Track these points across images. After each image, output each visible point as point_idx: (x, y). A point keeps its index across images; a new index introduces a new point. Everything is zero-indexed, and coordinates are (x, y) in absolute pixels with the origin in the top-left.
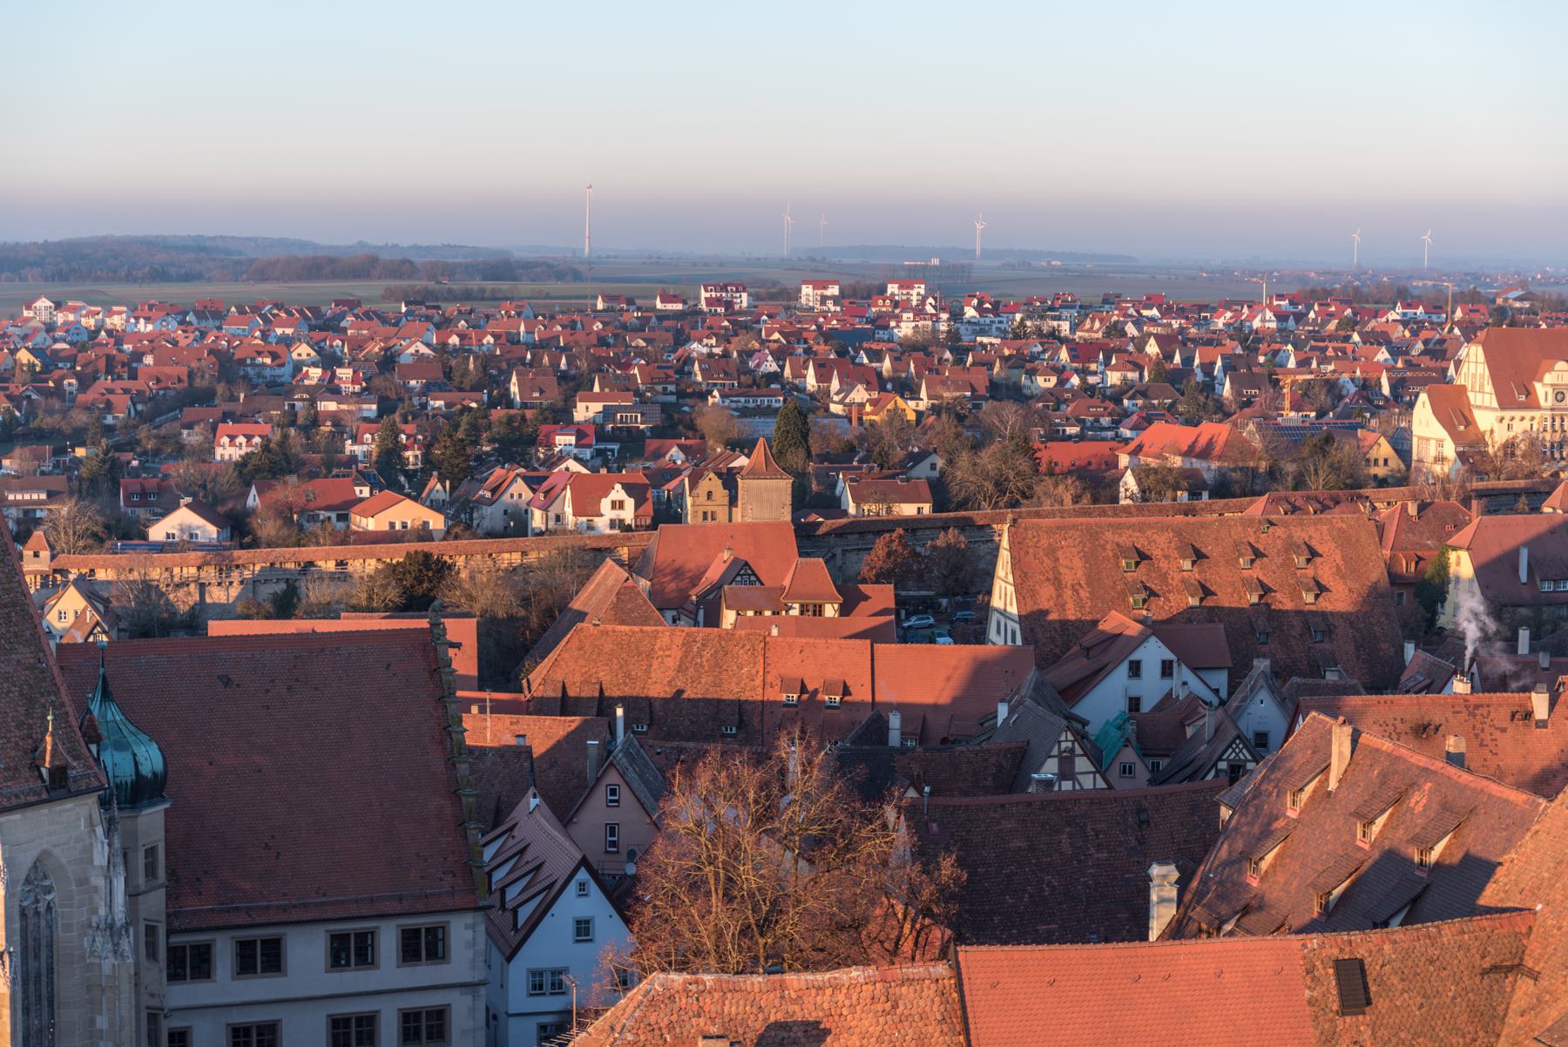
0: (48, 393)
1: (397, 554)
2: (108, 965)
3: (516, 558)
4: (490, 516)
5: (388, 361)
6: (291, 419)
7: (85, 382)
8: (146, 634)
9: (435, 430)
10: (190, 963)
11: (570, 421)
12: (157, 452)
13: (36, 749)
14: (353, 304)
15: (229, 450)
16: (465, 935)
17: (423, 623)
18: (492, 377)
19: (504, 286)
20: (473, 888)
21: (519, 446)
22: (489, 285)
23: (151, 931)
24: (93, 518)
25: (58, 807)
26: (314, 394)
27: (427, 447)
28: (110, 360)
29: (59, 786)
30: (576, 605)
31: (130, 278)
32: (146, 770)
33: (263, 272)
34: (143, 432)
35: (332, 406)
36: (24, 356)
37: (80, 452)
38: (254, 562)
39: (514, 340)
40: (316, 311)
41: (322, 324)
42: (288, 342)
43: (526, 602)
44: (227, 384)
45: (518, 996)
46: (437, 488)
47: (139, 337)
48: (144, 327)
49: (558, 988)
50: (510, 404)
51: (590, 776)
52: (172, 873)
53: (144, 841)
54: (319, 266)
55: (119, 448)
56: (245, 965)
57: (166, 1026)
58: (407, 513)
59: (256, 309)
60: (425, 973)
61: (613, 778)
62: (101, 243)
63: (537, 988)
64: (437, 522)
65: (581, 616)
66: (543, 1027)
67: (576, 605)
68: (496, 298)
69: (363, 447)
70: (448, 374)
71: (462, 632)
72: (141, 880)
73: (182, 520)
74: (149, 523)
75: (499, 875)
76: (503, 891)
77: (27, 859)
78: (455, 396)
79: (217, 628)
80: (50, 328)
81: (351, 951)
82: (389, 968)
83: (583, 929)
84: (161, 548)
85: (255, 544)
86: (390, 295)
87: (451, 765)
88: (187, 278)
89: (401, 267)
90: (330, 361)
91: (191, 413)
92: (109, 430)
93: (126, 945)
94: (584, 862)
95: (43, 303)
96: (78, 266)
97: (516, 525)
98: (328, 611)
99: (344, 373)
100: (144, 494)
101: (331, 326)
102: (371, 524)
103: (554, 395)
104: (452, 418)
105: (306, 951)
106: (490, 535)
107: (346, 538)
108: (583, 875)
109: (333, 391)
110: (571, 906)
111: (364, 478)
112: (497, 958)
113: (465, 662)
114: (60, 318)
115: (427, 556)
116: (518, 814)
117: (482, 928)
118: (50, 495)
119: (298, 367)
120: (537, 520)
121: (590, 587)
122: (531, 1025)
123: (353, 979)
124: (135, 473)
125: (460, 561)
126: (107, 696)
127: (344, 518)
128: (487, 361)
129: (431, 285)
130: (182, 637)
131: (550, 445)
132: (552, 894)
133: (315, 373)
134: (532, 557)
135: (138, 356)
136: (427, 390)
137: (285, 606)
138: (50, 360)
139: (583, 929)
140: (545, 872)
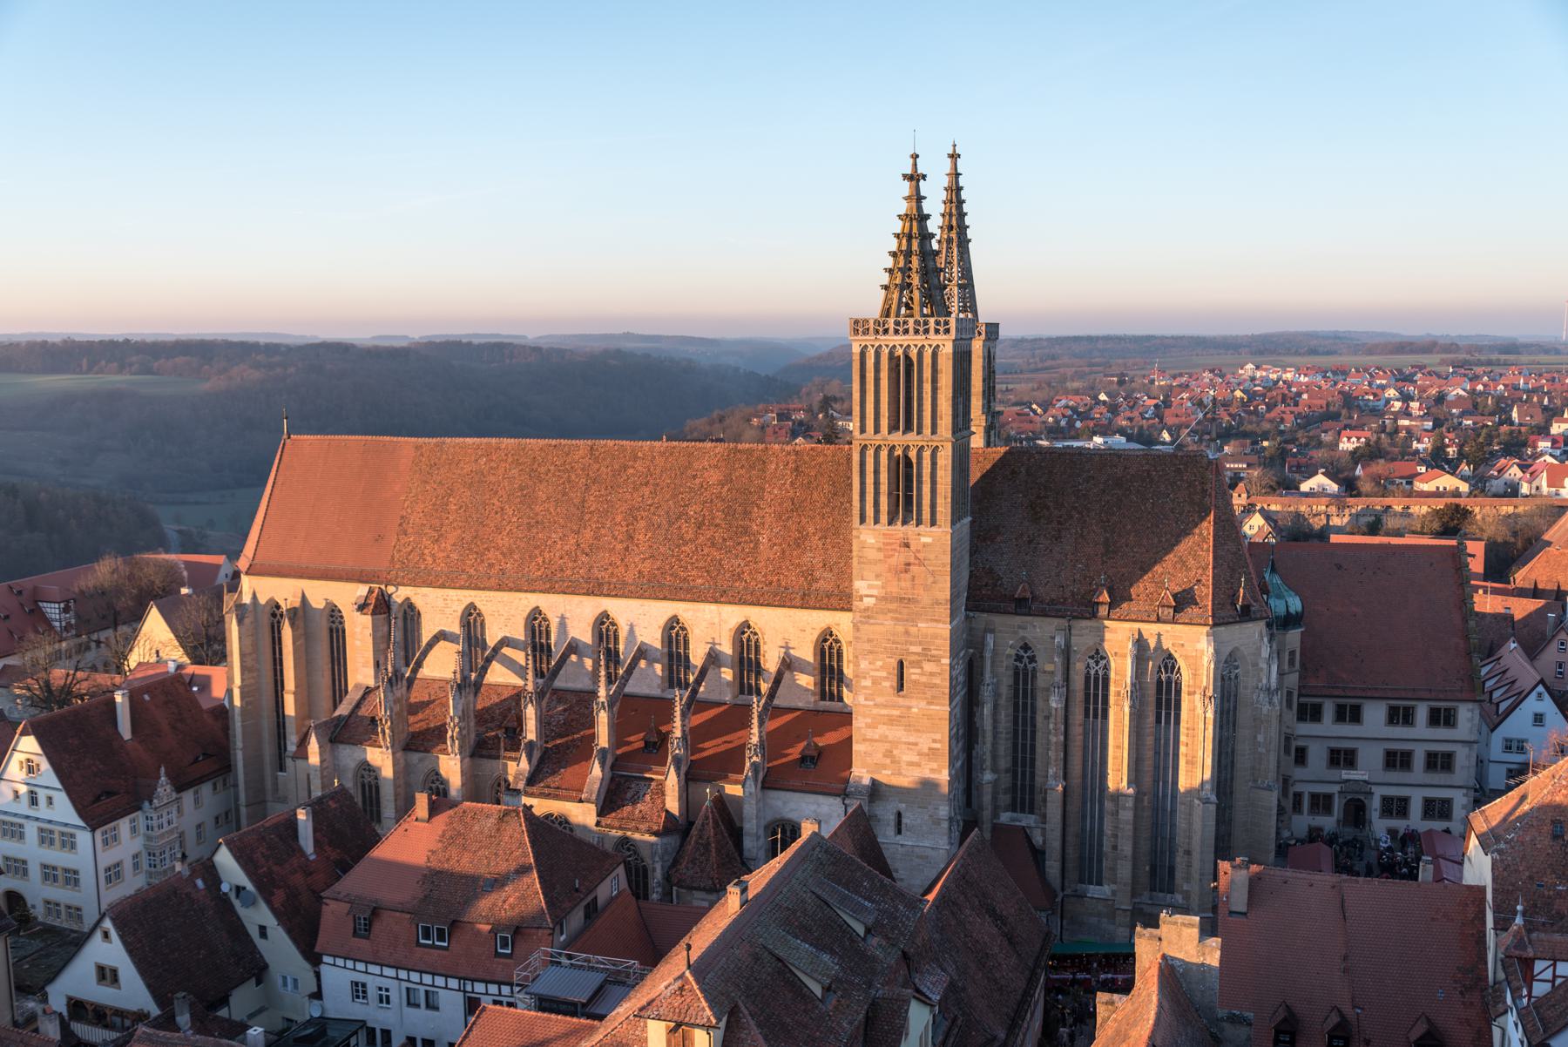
0: (1250, 413)
1: (1440, 504)
2: (1265, 709)
3: (1511, 509)
4: (1496, 485)
5: (1441, 399)
6: (1383, 429)
7: (1270, 407)
8: (1296, 540)
9: (1465, 437)
10: (1310, 713)
11: (1548, 434)
12: (1307, 445)
13: (1235, 595)
14: (1421, 368)
15: (1347, 445)
16: (1467, 715)
17: (1454, 543)
18: (1502, 408)
19: (1512, 357)
20: (1474, 690)
21: (1516, 447)
22: (1503, 357)
23: (1290, 694)
24: (1271, 478)
25: (1244, 625)
26: (1397, 416)
27: (1461, 447)
28: (1284, 396)
29: (1246, 615)
30: (1546, 537)
31: (1297, 353)
32: (1292, 610)
33: (1371, 350)
34: (1300, 434)
35: (1406, 422)
36: (1238, 394)
37: (1266, 444)
38: (1358, 504)
39: (1516, 388)
40: (1400, 371)
41: (1403, 378)
42: (1383, 388)
43: (1515, 534)
44: (1347, 411)
45: (1496, 750)
46: (1465, 468)
47: (1301, 384)
48: (1303, 379)
49: (1521, 749)
50: (1512, 423)
51: (1549, 634)
52: (1303, 665)
53: (1289, 648)
54: (1404, 347)
55: (1286, 442)
56: (1340, 716)
57: (1294, 744)
58: (1447, 482)
59: (1366, 370)
60: (1442, 733)
61: (1563, 636)
62: (1282, 335)
63: (1508, 748)
64: (1464, 487)
65: (1549, 544)
66: (1510, 771)
67: (1546, 537)
68: (1506, 364)
69: (1424, 445)
70: (1475, 406)
71: (1476, 548)
72: (1286, 667)
73: (1319, 481)
74: (1301, 482)
75: (1489, 684)
76: (1491, 693)
77: (1227, 650)
78: (1479, 418)
79: (1334, 539)
80: (1253, 379)
81: (1400, 716)
82: (1420, 726)
83: (1539, 719)
84: (1306, 495)
85: (1359, 495)
86: (1443, 362)
87: (1465, 620)
88: (1329, 353)
89: (1451, 347)
90: (1406, 398)
91: (1326, 425)
92: (1282, 432)
93: (1276, 700)
94: (1542, 682)
95: (1250, 366)
96: (1268, 347)
97: (1512, 491)
98: (1398, 533)
99: (1414, 405)
100: (1299, 466)
101: (1409, 379)
102: (1425, 487)
103: (1539, 419)
104: (1476, 430)
105: (1375, 715)
106: (1495, 496)
107: (1411, 494)
108: (1540, 688)
109: (1406, 413)
110: (1531, 705)
111: (1423, 462)
112: (1485, 729)
113: (1477, 565)
114: (1258, 374)
115: (1457, 506)
116: (1502, 651)
117: (1477, 712)
118: (1249, 465)
119: (1388, 401)
120: (1525, 489)
121: (1556, 527)
122: (1504, 768)
123: (1399, 731)
124: (1295, 455)
125: (1477, 510)
126: (1273, 570)
127: (1410, 483)
128: (1499, 399)
129: (1468, 357)
130: (1316, 542)
131: (1535, 447)
132: (1521, 698)
133: (1397, 405)
134: (1521, 509)
135: (1299, 394)
136: (1463, 415)
137: (1374, 529)
138: (1252, 395)
139: (1539, 719)
140: (1517, 684)
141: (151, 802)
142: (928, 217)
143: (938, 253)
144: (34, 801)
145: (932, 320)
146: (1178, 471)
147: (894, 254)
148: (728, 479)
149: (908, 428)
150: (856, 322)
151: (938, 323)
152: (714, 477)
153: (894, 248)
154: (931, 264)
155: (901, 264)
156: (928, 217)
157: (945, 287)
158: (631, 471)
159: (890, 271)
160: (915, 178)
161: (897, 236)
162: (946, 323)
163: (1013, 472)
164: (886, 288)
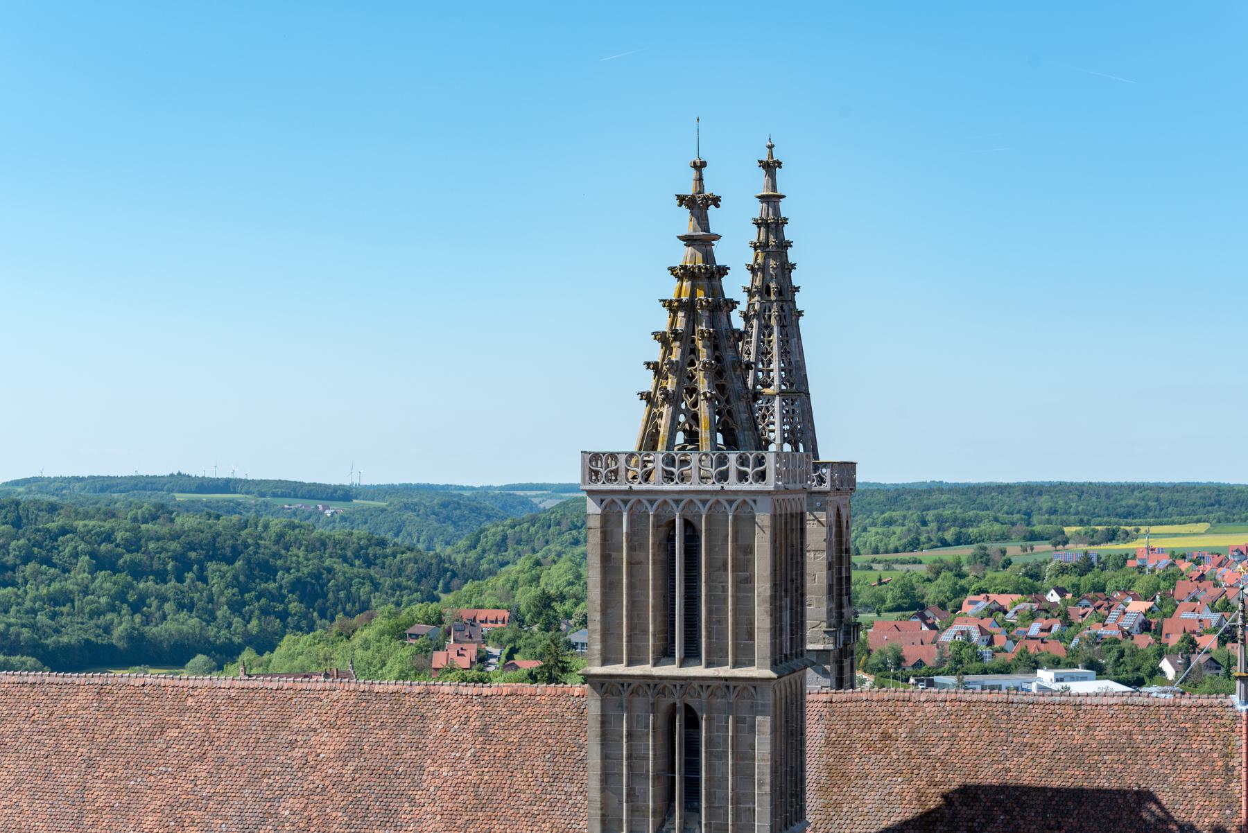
142: (723, 271)
143: (742, 335)
145: (733, 457)
146: (1183, 734)
147: (662, 338)
148: (354, 750)
149: (691, 654)
150: (595, 457)
151: (743, 461)
152: (329, 744)
153: (664, 327)
154: (729, 355)
155: (676, 356)
156: (723, 271)
157: (756, 396)
158: (173, 733)
159: (655, 367)
160: (699, 204)
161: (668, 304)
162: (760, 461)
163: (886, 736)
164: (648, 397)
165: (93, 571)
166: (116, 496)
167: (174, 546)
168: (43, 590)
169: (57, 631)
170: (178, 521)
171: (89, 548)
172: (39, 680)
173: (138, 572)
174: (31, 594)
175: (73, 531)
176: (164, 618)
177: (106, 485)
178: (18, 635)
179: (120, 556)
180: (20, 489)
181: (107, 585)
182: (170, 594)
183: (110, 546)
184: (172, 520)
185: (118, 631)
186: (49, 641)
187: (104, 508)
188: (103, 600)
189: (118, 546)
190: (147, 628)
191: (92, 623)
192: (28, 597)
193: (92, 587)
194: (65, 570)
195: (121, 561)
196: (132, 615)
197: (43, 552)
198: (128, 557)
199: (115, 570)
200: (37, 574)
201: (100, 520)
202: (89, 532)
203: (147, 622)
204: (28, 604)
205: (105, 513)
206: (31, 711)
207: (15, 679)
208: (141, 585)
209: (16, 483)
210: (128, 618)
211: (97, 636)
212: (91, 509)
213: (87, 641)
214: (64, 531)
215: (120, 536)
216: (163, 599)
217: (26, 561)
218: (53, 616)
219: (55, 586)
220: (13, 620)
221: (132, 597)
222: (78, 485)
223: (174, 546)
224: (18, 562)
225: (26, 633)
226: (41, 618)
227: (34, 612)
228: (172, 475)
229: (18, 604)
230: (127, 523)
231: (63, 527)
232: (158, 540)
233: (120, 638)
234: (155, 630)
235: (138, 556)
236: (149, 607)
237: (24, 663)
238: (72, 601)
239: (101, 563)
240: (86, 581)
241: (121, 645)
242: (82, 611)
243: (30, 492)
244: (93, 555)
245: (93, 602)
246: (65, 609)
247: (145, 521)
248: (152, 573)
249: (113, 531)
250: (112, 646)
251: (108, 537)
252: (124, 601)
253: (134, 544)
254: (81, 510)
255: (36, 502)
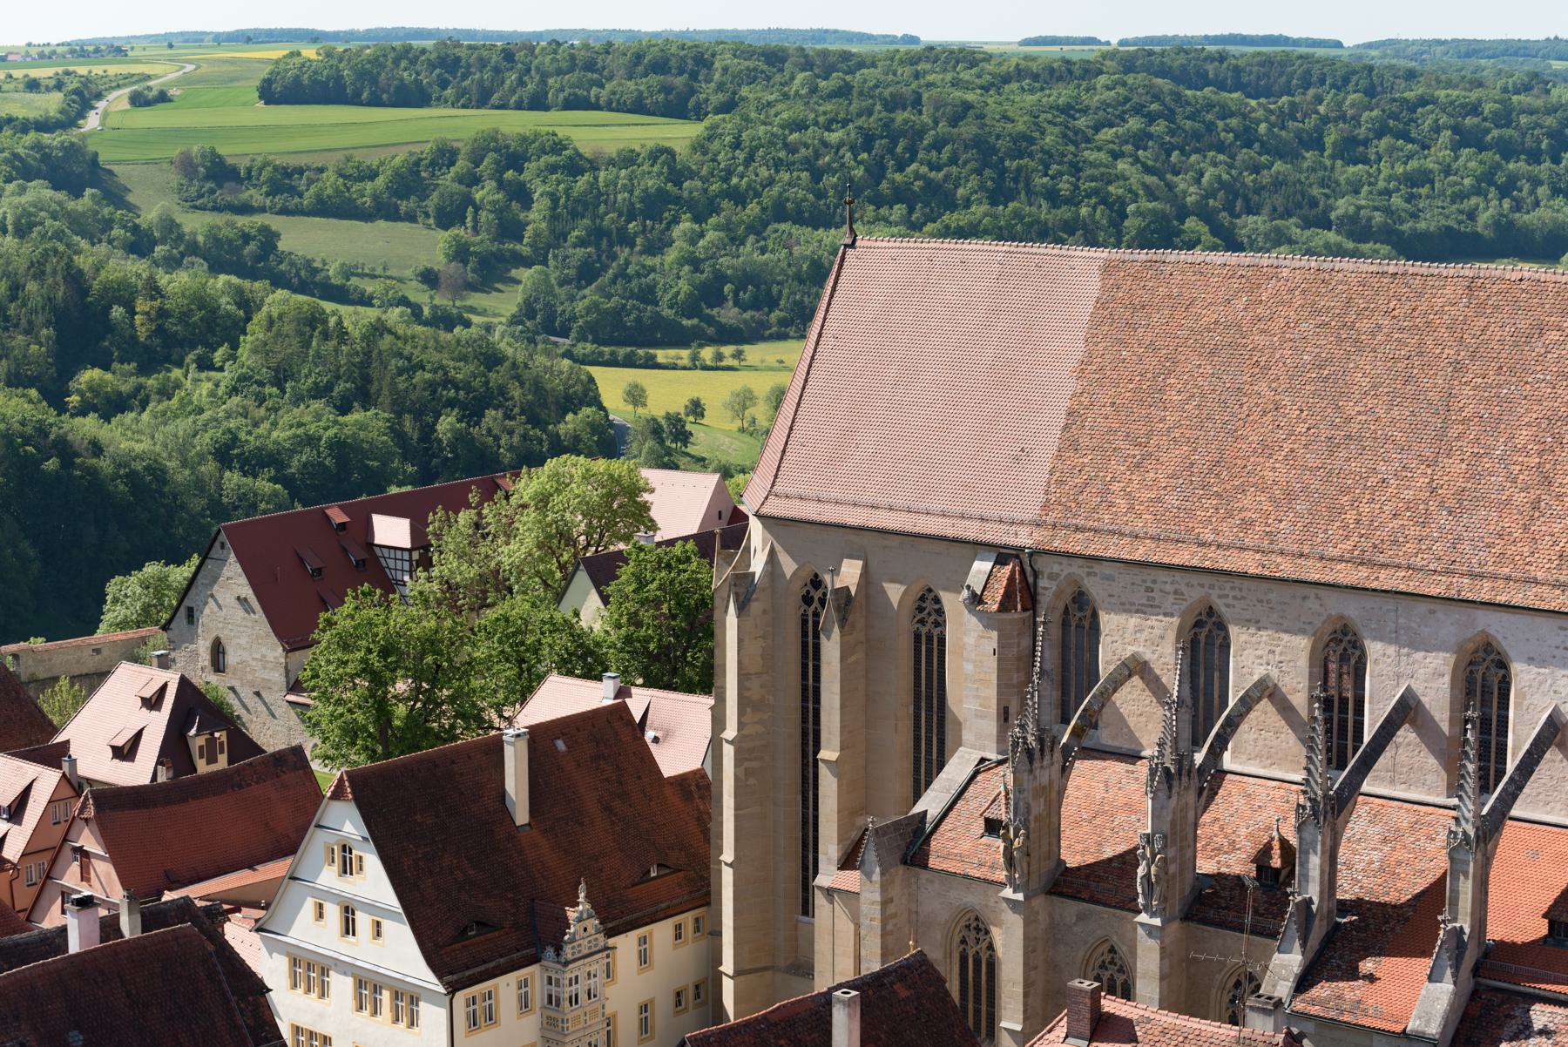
141: (558, 950)
144: (349, 928)
165: (1456, 147)
166: (1483, 62)
167: (1549, 121)
168: (1400, 169)
169: (1414, 216)
170: (1555, 92)
171: (1452, 121)
172: (1401, 270)
173: (1508, 150)
174: (1385, 172)
175: (1434, 101)
176: (1537, 204)
177: (1472, 49)
178: (1370, 219)
179: (1488, 131)
180: (1374, 53)
181: (1472, 164)
182: (1544, 176)
183: (1476, 120)
184: (1548, 92)
185: (1484, 218)
186: (1406, 227)
187: (1469, 76)
188: (1467, 182)
189: (1485, 119)
190: (1517, 215)
191: (1455, 207)
192: (1382, 176)
193: (1455, 166)
194: (1425, 147)
195: (1489, 137)
196: (1500, 200)
197: (1400, 123)
198: (1495, 133)
199: (1482, 148)
200: (1391, 150)
201: (1465, 89)
202: (1452, 103)
203: (1518, 206)
204: (1381, 184)
205: (1471, 82)
206: (1392, 306)
207: (1374, 268)
208: (1511, 166)
209: (1370, 46)
210: (1495, 202)
211: (1460, 222)
212: (1455, 77)
213: (1449, 228)
214: (1423, 102)
215: (1488, 108)
216: (1536, 182)
217: (1379, 136)
218: (1410, 198)
219: (1413, 164)
220: (1363, 202)
221: (1501, 179)
222: (1440, 49)
223: (1549, 121)
224: (1371, 135)
225: (1378, 217)
226: (1396, 201)
227: (1387, 193)
228: (1548, 39)
229: (1370, 184)
230: (1496, 93)
231: (1422, 97)
232: (1532, 114)
233: (1486, 226)
234: (1526, 217)
235: (1508, 132)
236: (1520, 190)
237: (1376, 251)
238: (1432, 182)
239: (1464, 139)
240: (1448, 160)
241: (1488, 233)
242: (1443, 193)
243: (1384, 56)
244: (1456, 129)
245: (1456, 184)
246: (1424, 191)
247: (1517, 92)
248: (1523, 153)
249: (1480, 101)
250: (1476, 235)
251: (1475, 109)
252: (1492, 183)
253: (1505, 118)
254: (1443, 77)
255: (1392, 67)
